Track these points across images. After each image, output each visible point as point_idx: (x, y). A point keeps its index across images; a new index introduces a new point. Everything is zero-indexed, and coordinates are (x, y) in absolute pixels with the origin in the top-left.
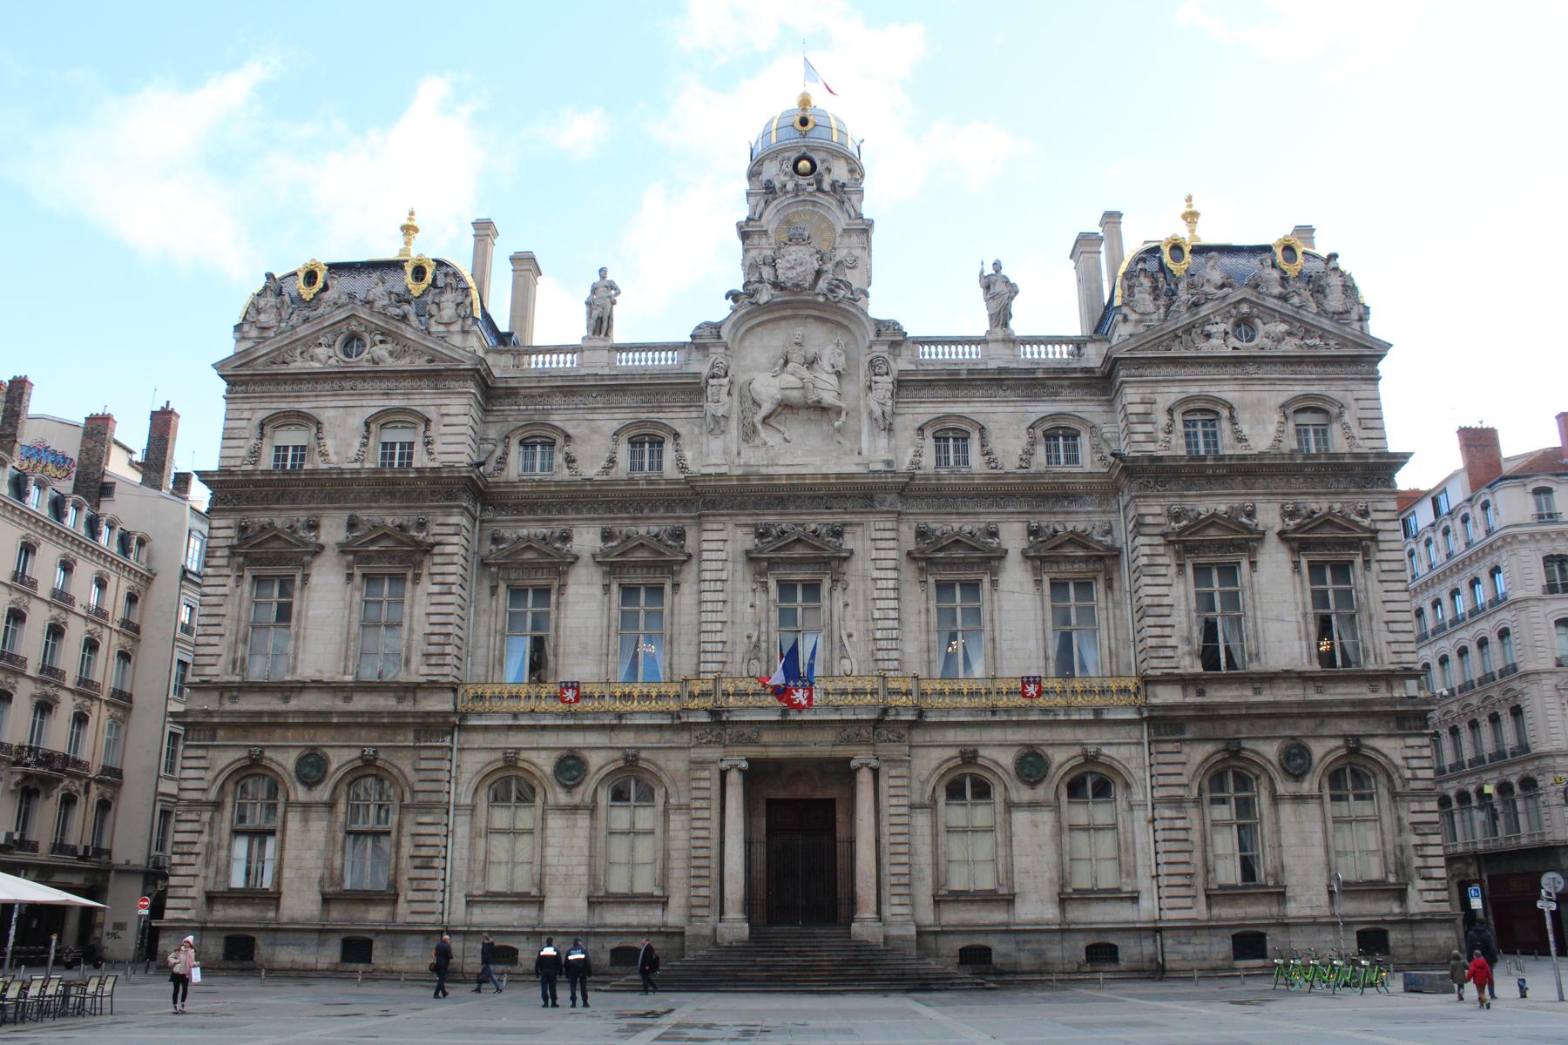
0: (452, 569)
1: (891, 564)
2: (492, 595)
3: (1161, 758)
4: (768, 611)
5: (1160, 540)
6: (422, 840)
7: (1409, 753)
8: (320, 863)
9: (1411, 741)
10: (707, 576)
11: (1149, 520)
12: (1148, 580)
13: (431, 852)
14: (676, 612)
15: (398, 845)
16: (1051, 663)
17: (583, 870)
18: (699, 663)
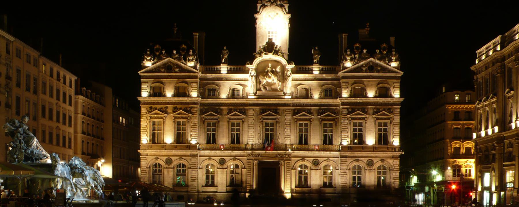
0: (196, 120)
1: (289, 119)
2: (203, 124)
3: (342, 163)
4: (262, 129)
5: (347, 117)
6: (193, 176)
7: (394, 163)
8: (172, 180)
9: (395, 161)
10: (250, 121)
11: (344, 112)
12: (343, 125)
13: (195, 179)
14: (243, 128)
15: (188, 177)
16: (322, 141)
17: (225, 182)
18: (248, 139)
